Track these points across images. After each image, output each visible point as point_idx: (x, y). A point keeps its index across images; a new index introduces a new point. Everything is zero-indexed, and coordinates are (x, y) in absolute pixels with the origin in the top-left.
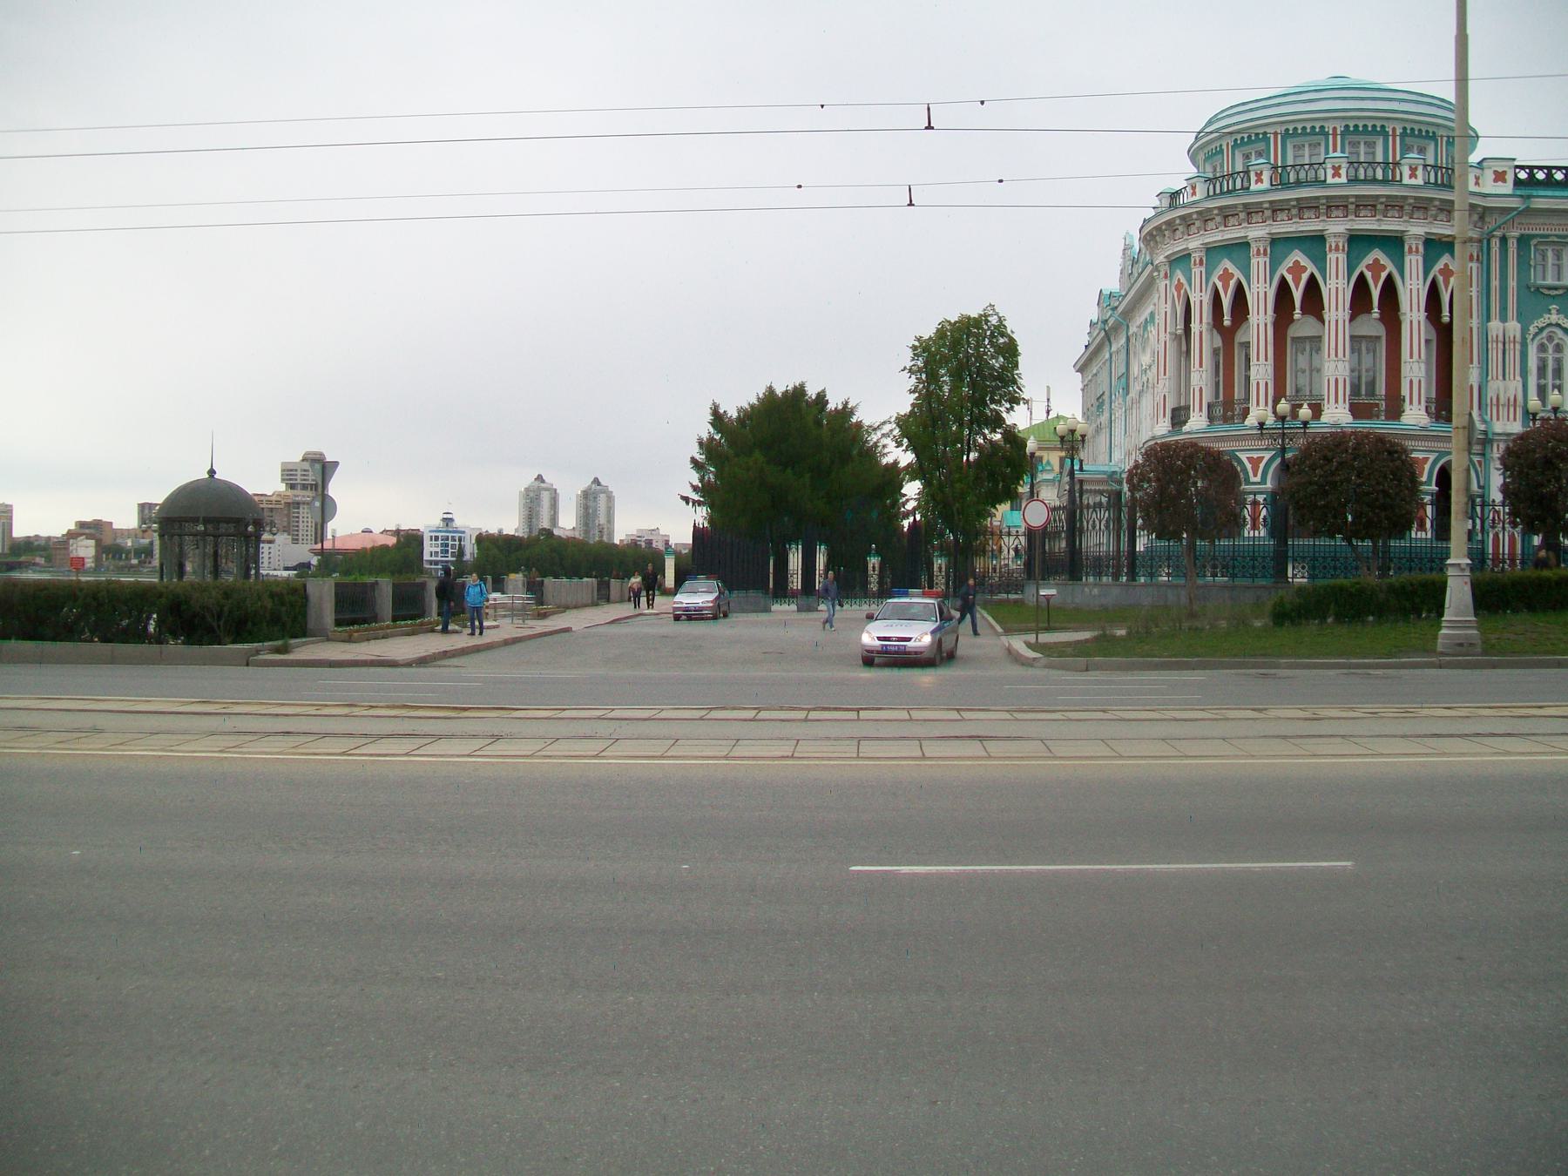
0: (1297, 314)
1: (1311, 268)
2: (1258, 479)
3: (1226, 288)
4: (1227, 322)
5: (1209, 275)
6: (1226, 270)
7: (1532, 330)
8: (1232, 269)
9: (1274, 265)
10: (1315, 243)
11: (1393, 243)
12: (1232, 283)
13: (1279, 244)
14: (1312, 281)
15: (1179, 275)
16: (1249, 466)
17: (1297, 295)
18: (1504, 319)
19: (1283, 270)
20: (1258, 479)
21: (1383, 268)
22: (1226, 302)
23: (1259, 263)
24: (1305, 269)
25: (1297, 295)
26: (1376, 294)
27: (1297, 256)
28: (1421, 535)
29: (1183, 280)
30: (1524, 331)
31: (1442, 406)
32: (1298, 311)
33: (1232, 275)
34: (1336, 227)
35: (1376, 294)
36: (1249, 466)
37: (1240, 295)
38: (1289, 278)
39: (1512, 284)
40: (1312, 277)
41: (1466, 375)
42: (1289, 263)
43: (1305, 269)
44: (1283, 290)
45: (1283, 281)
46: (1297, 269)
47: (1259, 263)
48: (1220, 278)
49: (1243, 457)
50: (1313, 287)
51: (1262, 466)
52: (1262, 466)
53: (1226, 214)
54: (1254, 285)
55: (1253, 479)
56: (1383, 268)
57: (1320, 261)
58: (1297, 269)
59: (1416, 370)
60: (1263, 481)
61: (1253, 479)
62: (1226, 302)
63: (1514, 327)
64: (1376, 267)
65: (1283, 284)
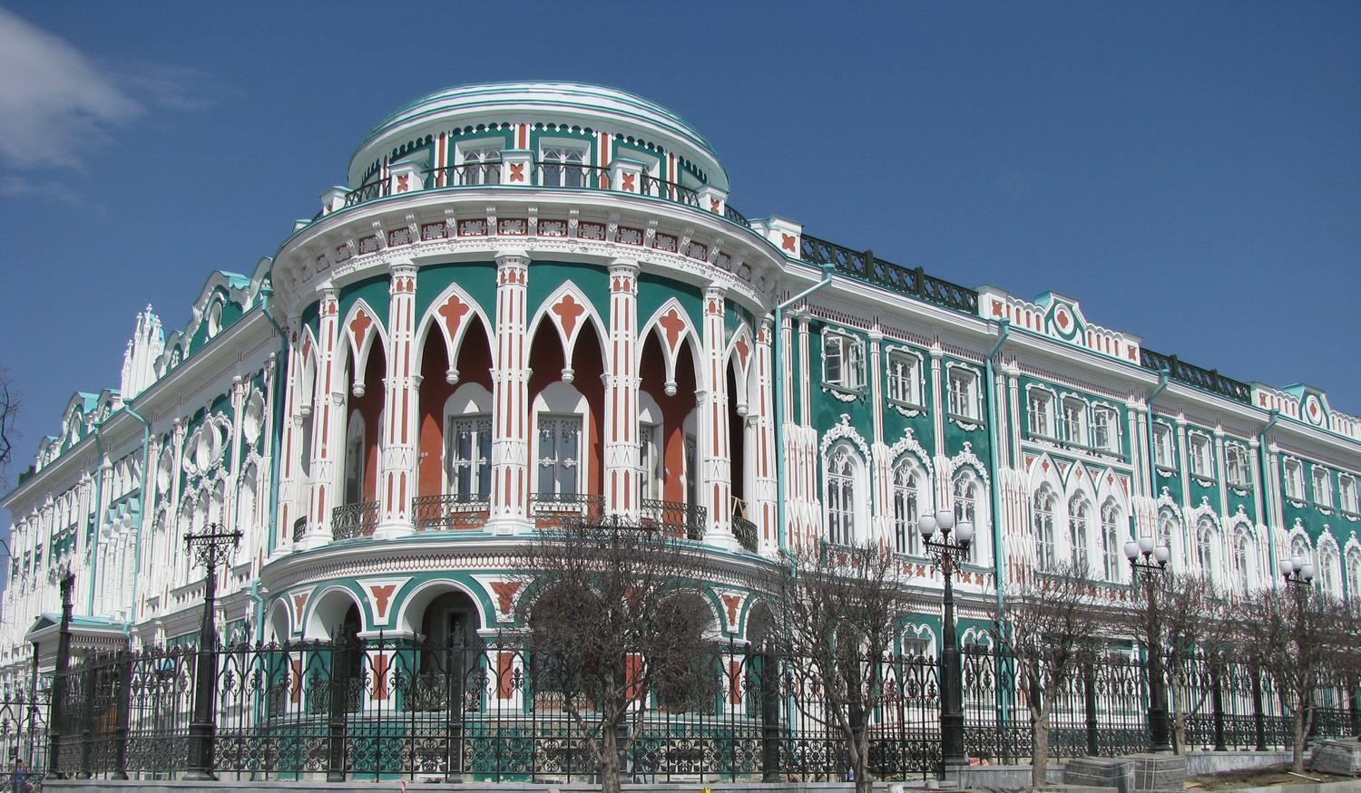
0: (568, 373)
1: (589, 310)
3: (453, 328)
4: (452, 375)
5: (422, 305)
6: (454, 300)
7: (826, 441)
8: (464, 298)
9: (536, 296)
10: (594, 274)
11: (691, 291)
12: (465, 320)
13: (545, 271)
15: (361, 305)
17: (569, 346)
18: (797, 421)
19: (547, 307)
21: (681, 326)
22: (453, 347)
23: (512, 294)
24: (580, 310)
25: (569, 346)
26: (672, 358)
27: (568, 289)
29: (370, 312)
30: (820, 441)
31: (744, 531)
32: (569, 367)
33: (465, 308)
34: (626, 255)
35: (672, 358)
37: (476, 341)
38: (557, 320)
39: (805, 378)
40: (589, 324)
41: (759, 491)
42: (557, 297)
43: (580, 310)
44: (546, 339)
45: (546, 320)
46: (569, 309)
47: (512, 294)
48: (443, 311)
49: (485, 581)
50: (589, 340)
53: (470, 220)
54: (505, 326)
56: (681, 326)
57: (601, 300)
58: (569, 309)
59: (714, 470)
62: (453, 347)
63: (807, 434)
64: (672, 323)
65: (546, 328)
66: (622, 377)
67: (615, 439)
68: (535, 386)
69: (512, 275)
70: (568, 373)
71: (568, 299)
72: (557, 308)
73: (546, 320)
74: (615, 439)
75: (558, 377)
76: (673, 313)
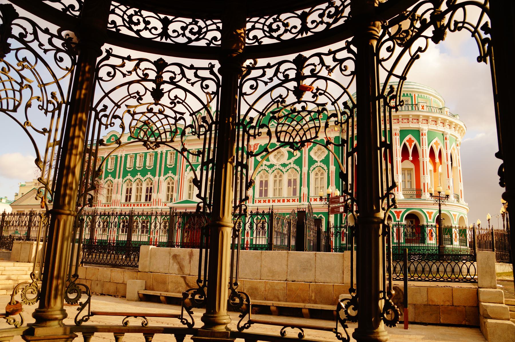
0: (411, 158)
1: (416, 142)
2: (399, 220)
13: (403, 133)
14: (415, 148)
16: (396, 215)
17: (410, 151)
19: (405, 141)
20: (399, 220)
24: (413, 141)
25: (410, 151)
28: (431, 242)
36: (396, 215)
38: (407, 144)
40: (415, 145)
42: (407, 138)
43: (413, 141)
44: (405, 150)
45: (405, 144)
46: (410, 141)
50: (415, 149)
51: (401, 214)
52: (401, 214)
55: (397, 220)
58: (410, 141)
60: (402, 220)
61: (397, 220)
66: (425, 158)
67: (424, 174)
68: (402, 161)
69: (396, 134)
70: (411, 158)
71: (410, 138)
72: (407, 141)
73: (405, 145)
74: (424, 174)
75: (408, 159)
76: (437, 141)
